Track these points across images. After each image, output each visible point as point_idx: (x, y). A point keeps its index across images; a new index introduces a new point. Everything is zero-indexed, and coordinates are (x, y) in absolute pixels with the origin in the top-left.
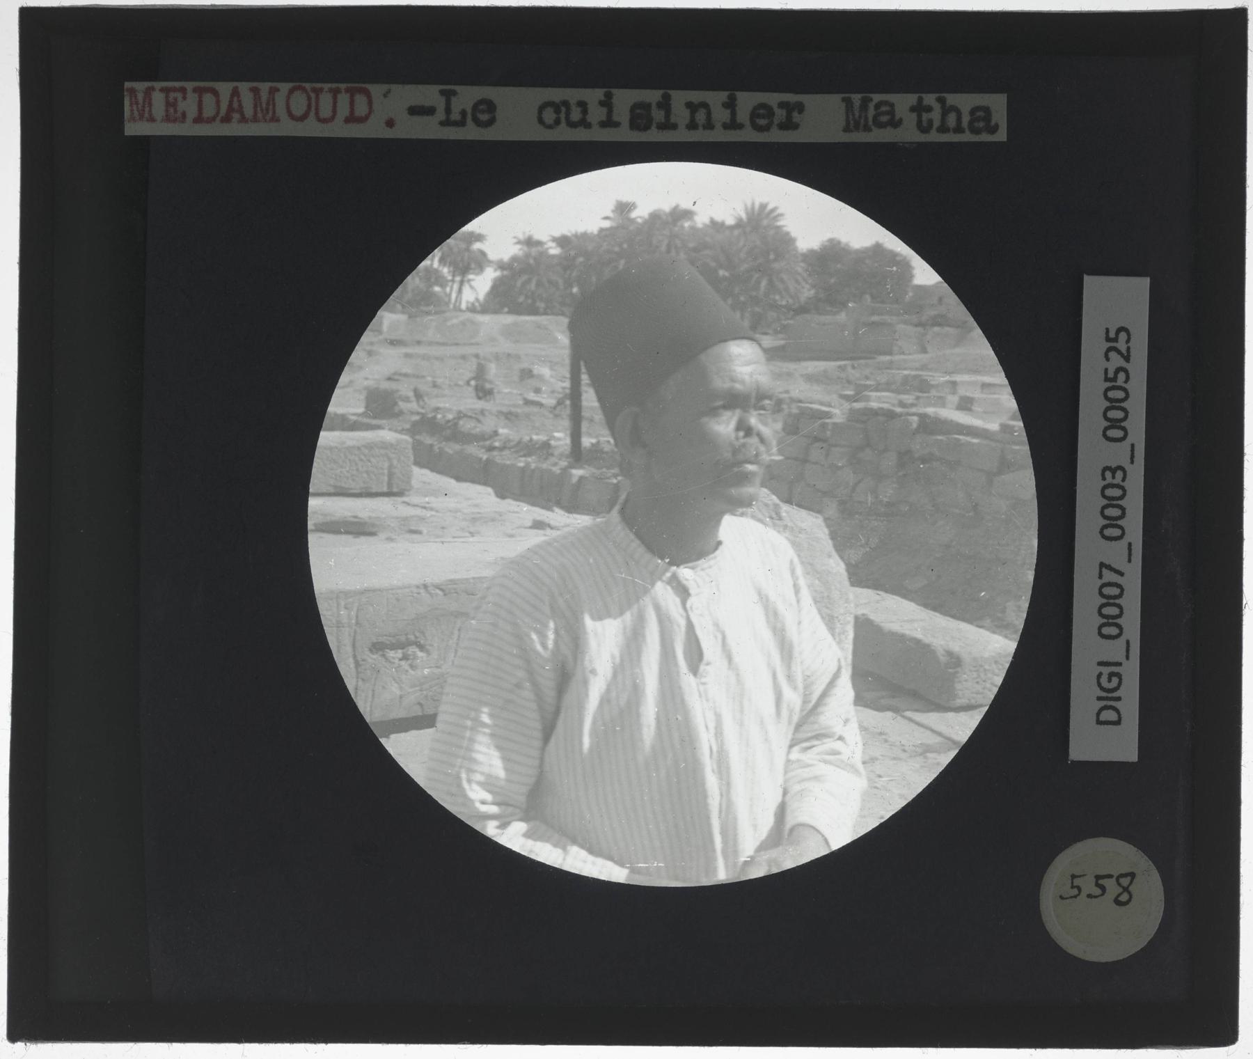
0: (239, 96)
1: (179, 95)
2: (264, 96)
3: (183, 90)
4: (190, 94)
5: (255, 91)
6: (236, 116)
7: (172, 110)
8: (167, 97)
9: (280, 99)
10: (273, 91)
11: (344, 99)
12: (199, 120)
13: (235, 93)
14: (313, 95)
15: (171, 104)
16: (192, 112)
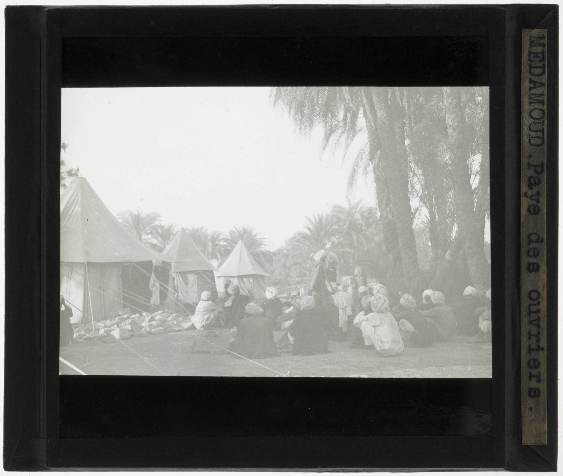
0: (540, 86)
1: (541, 58)
2: (541, 98)
3: (543, 60)
4: (543, 63)
5: (542, 95)
6: (532, 86)
7: (535, 55)
8: (540, 53)
9: (540, 106)
10: (542, 103)
11: (540, 134)
12: (531, 67)
13: (543, 85)
14: (539, 121)
15: (536, 54)
16: (533, 65)
